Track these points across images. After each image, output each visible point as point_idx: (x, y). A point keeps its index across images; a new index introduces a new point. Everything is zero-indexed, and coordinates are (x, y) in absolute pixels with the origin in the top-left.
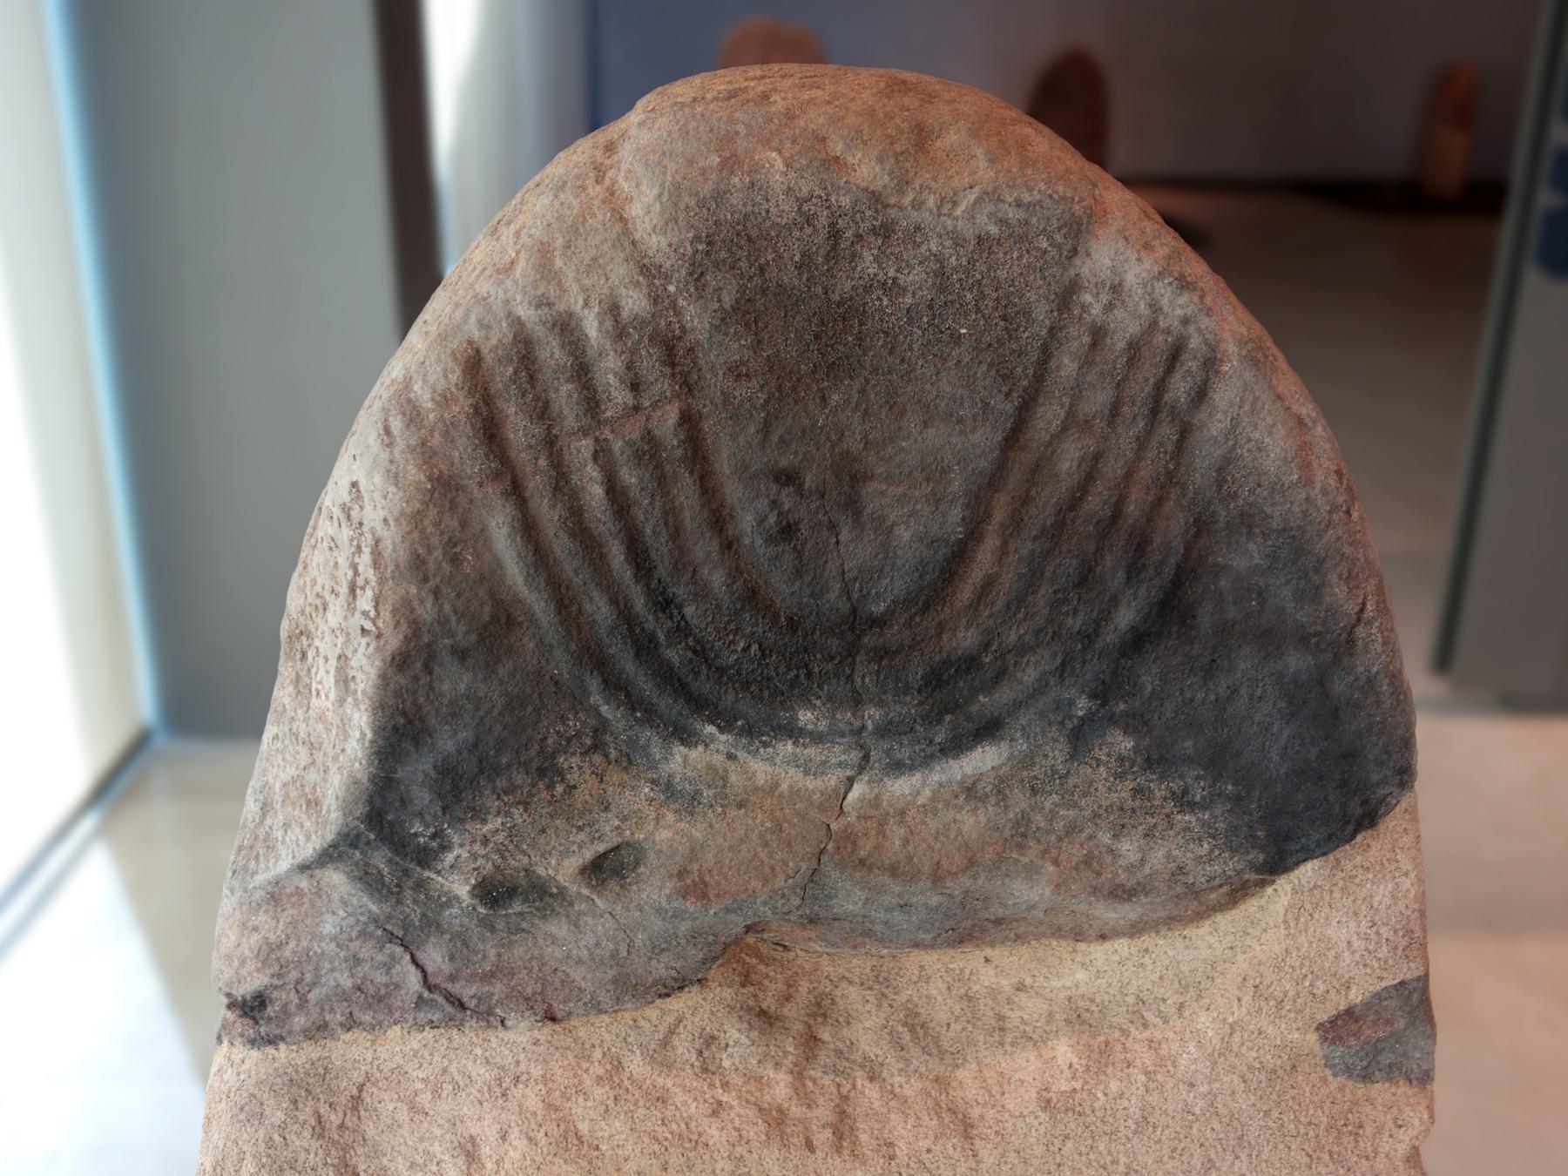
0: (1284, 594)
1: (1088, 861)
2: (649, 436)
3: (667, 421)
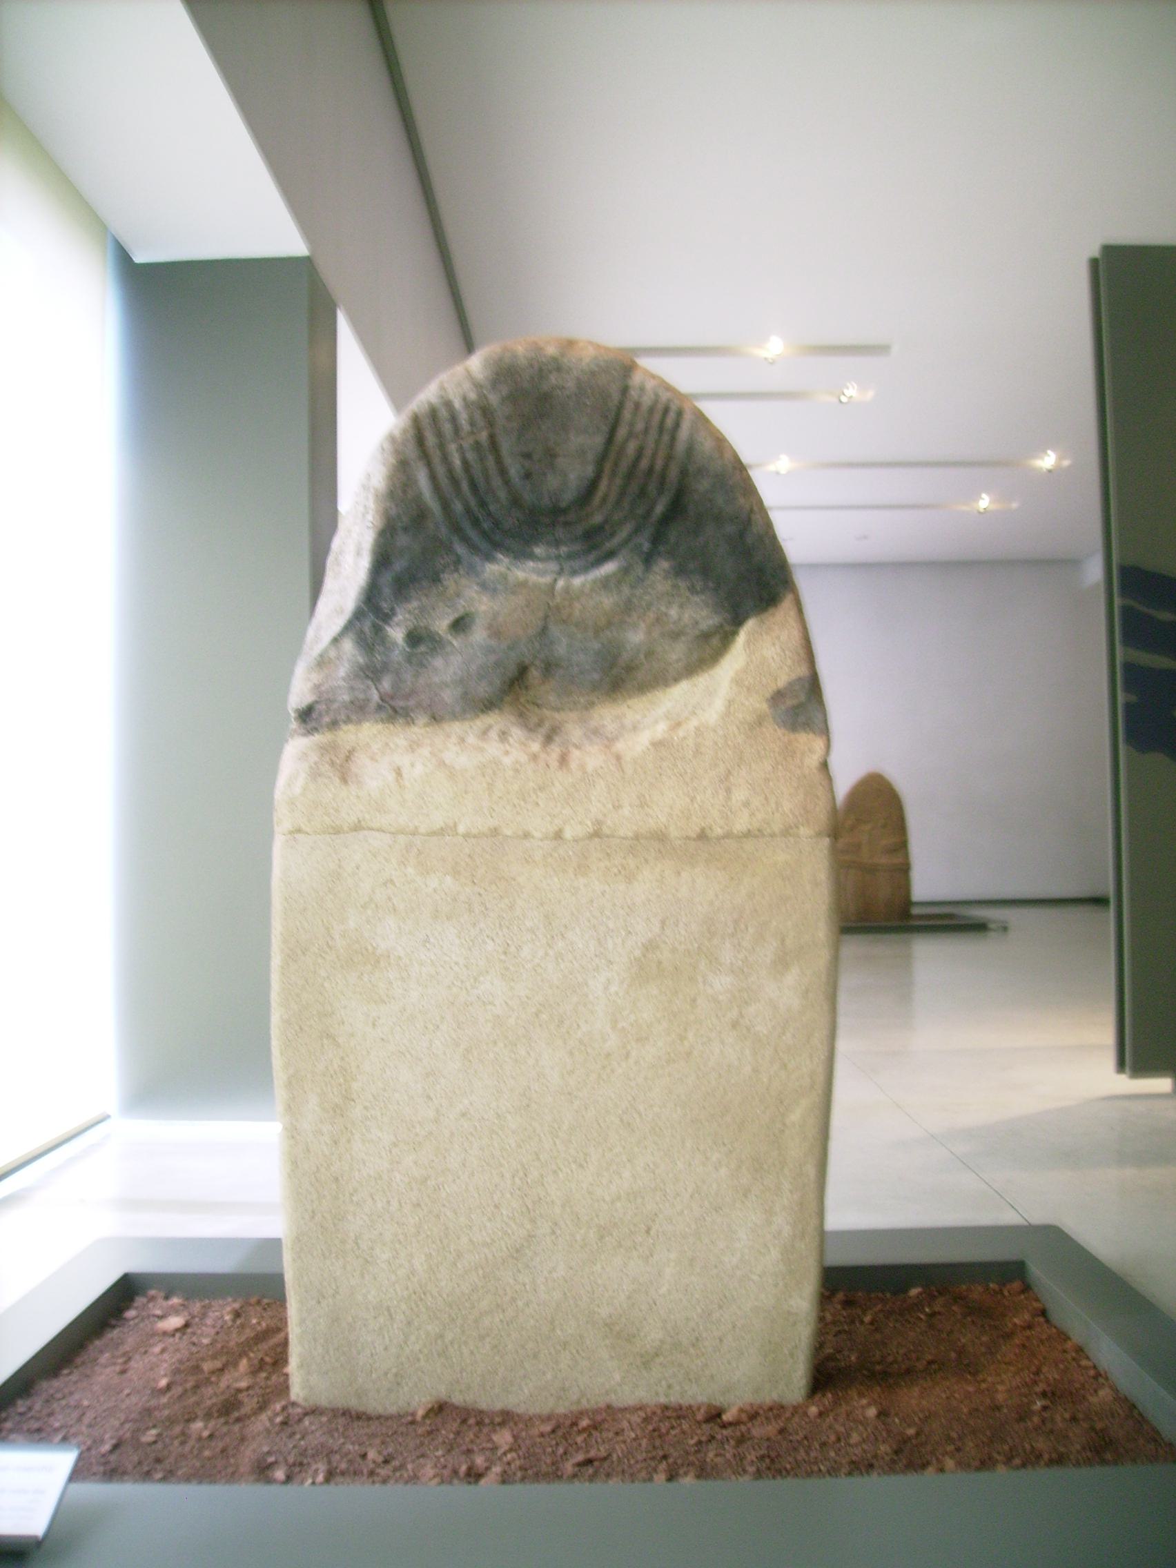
0: (720, 500)
1: (658, 620)
2: (477, 443)
3: (483, 436)
